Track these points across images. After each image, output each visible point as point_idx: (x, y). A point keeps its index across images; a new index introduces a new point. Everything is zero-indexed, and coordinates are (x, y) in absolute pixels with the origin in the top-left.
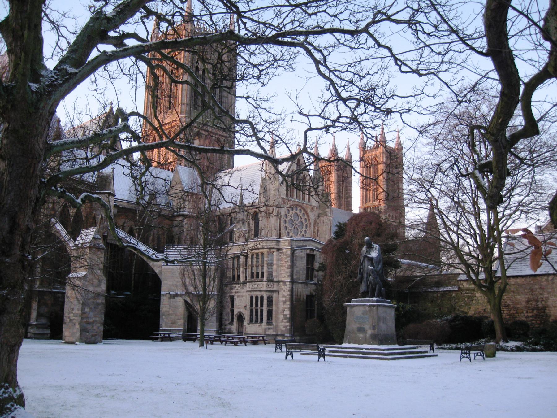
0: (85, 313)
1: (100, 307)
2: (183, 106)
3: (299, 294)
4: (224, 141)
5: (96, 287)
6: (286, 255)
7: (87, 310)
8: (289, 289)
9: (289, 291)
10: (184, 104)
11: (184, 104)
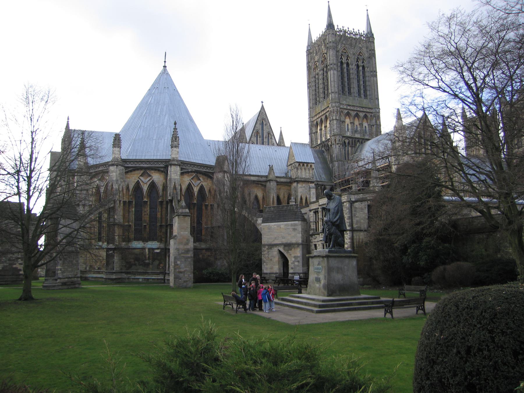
0: (178, 265)
1: (189, 260)
2: (333, 94)
3: (361, 241)
4: (371, 116)
5: (185, 245)
6: (346, 208)
7: (179, 262)
9: (350, 239)
10: (333, 93)
11: (333, 93)
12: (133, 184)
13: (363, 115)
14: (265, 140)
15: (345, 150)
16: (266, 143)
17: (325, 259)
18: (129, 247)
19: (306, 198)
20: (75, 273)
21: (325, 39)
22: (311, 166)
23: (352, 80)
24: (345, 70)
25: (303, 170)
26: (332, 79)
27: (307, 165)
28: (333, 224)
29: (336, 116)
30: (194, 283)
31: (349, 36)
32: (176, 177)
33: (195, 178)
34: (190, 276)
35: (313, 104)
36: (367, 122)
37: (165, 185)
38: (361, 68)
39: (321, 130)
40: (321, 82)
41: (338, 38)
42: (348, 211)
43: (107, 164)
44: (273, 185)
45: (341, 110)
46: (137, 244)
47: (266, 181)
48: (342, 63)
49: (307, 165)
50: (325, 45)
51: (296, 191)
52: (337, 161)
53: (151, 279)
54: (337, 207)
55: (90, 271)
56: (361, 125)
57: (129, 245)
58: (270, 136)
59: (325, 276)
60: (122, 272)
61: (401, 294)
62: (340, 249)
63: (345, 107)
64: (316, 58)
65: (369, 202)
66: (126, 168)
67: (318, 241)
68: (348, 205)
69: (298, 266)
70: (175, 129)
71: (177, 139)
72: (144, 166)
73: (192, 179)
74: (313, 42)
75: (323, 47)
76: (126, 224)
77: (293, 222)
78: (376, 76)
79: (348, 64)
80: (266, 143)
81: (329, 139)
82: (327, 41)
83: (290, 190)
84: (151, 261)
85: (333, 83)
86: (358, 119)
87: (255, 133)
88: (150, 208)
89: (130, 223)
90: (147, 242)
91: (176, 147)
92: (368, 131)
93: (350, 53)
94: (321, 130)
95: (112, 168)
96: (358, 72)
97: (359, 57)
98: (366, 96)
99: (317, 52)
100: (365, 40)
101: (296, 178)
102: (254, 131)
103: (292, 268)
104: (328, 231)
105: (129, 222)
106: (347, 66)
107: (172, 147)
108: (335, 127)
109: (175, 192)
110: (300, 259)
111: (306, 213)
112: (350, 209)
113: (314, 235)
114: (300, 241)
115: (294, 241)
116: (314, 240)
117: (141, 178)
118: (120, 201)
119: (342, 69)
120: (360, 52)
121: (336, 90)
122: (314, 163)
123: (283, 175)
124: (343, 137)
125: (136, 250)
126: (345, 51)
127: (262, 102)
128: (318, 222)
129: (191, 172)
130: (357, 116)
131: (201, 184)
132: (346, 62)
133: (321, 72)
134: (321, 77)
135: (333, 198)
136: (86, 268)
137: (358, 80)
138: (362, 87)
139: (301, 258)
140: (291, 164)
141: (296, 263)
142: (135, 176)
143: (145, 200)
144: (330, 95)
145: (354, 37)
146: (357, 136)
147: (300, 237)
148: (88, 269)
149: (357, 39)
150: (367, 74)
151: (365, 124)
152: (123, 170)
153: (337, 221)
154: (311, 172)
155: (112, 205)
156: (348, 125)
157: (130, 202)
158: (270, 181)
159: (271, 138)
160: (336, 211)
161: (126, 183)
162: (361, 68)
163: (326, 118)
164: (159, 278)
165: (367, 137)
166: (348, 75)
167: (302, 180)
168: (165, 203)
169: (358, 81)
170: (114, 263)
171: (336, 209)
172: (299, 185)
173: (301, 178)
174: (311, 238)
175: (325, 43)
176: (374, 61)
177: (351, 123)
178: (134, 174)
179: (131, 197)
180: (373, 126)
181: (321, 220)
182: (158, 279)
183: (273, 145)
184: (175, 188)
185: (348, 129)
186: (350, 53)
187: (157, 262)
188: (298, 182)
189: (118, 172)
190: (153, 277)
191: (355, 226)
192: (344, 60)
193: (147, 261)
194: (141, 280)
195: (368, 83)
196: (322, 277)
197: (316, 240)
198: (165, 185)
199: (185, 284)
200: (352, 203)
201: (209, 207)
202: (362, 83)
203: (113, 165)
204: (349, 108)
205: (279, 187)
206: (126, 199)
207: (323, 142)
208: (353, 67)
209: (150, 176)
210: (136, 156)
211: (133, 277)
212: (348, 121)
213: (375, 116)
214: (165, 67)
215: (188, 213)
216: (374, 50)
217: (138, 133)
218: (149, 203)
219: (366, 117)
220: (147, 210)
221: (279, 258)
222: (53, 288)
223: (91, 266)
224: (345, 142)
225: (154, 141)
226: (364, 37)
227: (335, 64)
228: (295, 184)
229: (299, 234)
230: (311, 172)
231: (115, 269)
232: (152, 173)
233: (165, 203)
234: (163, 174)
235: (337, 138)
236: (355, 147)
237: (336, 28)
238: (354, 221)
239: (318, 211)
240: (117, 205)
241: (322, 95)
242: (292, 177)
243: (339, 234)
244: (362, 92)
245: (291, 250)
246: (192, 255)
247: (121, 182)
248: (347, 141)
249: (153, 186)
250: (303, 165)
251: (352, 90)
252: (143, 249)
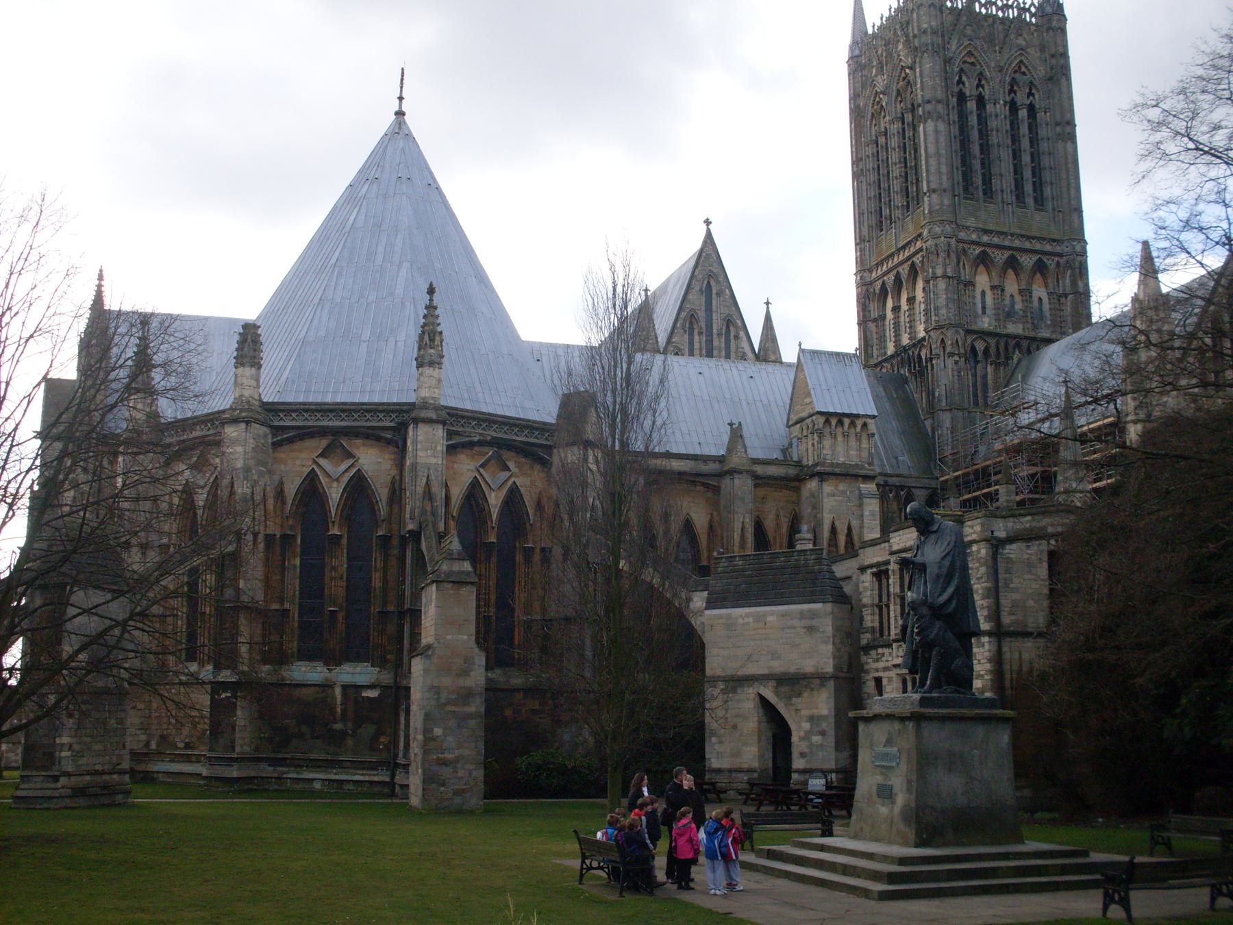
0: (434, 739)
1: (472, 723)
2: (934, 196)
3: (1025, 668)
4: (1058, 264)
5: (459, 675)
6: (978, 560)
7: (438, 731)
8: (987, 654)
9: (990, 661)
10: (934, 191)
11: (934, 191)
12: (298, 481)
13: (1032, 263)
14: (716, 343)
15: (975, 375)
16: (720, 351)
17: (910, 725)
18: (283, 679)
19: (849, 529)
20: (114, 759)
21: (908, 23)
22: (865, 425)
23: (994, 152)
24: (973, 120)
25: (840, 438)
26: (931, 149)
27: (853, 424)
28: (937, 612)
29: (945, 266)
30: (485, 798)
31: (984, 11)
32: (433, 461)
33: (492, 462)
34: (474, 774)
35: (870, 227)
36: (1046, 286)
37: (397, 486)
38: (1023, 113)
39: (896, 309)
40: (895, 156)
41: (949, 19)
42: (983, 569)
43: (216, 420)
44: (741, 486)
45: (961, 246)
46: (308, 672)
47: (720, 475)
48: (962, 97)
49: (853, 424)
50: (907, 42)
51: (816, 507)
52: (951, 410)
53: (348, 781)
54: (949, 559)
55: (160, 754)
56: (1026, 293)
57: (284, 674)
58: (732, 328)
59: (909, 782)
60: (259, 760)
61: (1157, 843)
62: (959, 692)
63: (974, 237)
64: (881, 82)
65: (1053, 542)
66: (276, 430)
67: (886, 669)
68: (983, 551)
69: (822, 746)
70: (431, 307)
71: (437, 338)
72: (331, 424)
73: (483, 466)
74: (870, 31)
75: (900, 46)
76: (275, 606)
77: (806, 606)
78: (1072, 137)
79: (981, 101)
80: (720, 351)
81: (924, 339)
82: (913, 29)
83: (798, 503)
84: (350, 725)
85: (933, 162)
86: (1017, 275)
87: (685, 320)
88: (350, 559)
89: (287, 606)
90: (339, 664)
91: (431, 364)
92: (1047, 313)
93: (988, 66)
94: (896, 309)
95: (231, 431)
96: (1014, 124)
97: (1017, 76)
98: (1040, 202)
99: (881, 63)
100: (1036, 25)
101: (816, 465)
102: (683, 315)
103: (802, 755)
104: (918, 634)
105: (281, 600)
106: (978, 109)
107: (420, 366)
108: (942, 301)
109: (429, 509)
110: (829, 726)
111: (849, 578)
112: (990, 563)
113: (876, 647)
114: (829, 669)
115: (808, 666)
116: (874, 665)
117: (322, 462)
118: (255, 535)
119: (963, 116)
120: (1021, 62)
121: (946, 184)
122: (874, 417)
123: (776, 455)
124: (969, 332)
125: (304, 690)
126: (972, 60)
127: (708, 222)
128: (888, 606)
129: (481, 443)
130: (1012, 263)
131: (510, 483)
132: (975, 92)
133: (896, 127)
134: (894, 142)
135: (935, 528)
136: (147, 744)
137: (1014, 151)
138: (1027, 173)
139: (832, 720)
140: (801, 421)
141: (816, 739)
142: (304, 455)
143: (335, 531)
144: (926, 199)
145: (1000, 14)
146: (1014, 328)
147: (830, 654)
148: (153, 746)
149: (1012, 21)
150: (1043, 132)
151: (1039, 292)
152: (265, 436)
153: (949, 601)
154: (865, 445)
155: (231, 548)
156: (983, 293)
157: (287, 539)
158: (733, 472)
159: (737, 337)
160: (945, 570)
161: (276, 478)
162: (1023, 113)
163: (914, 272)
164: (376, 779)
165: (1045, 333)
166: (984, 133)
167: (837, 470)
168: (395, 542)
169: (1016, 155)
170: (234, 728)
171: (947, 563)
172: (828, 488)
173: (832, 465)
174: (864, 658)
175: (907, 36)
176: (1064, 89)
177: (993, 288)
178: (300, 451)
179: (291, 522)
180: (1066, 296)
181: (898, 601)
182: (371, 783)
183: (743, 357)
184: (428, 494)
185: (984, 308)
186: (988, 66)
187: (368, 730)
188: (823, 476)
189: (251, 443)
190: (356, 778)
191: (1006, 620)
192: (969, 88)
193: (338, 726)
194: (317, 785)
195: (1046, 161)
196: (898, 782)
197: (881, 665)
198: (397, 486)
199: (457, 800)
200: (996, 545)
201: (537, 557)
202: (1026, 158)
203: (235, 421)
204: (985, 239)
205: (762, 492)
206: (274, 529)
207: (905, 349)
208: (998, 110)
209: (349, 455)
210: (307, 392)
211: (295, 776)
212: (983, 281)
213: (1069, 265)
214: (400, 114)
215: (468, 573)
216: (1065, 55)
217: (315, 322)
218: (344, 542)
219: (1040, 268)
220: (339, 562)
221: (759, 722)
222: (45, 805)
223: (163, 738)
224: (973, 349)
225: (364, 346)
226: (1032, 15)
227: (939, 102)
228: (812, 485)
229: (826, 643)
230: (865, 445)
231: (238, 749)
232: (358, 448)
233: (395, 542)
234: (392, 449)
235: (950, 335)
236: (1006, 365)
238: (1005, 602)
240: (247, 548)
241: (899, 200)
242: (805, 462)
243: (956, 644)
244: (1028, 188)
245: (799, 695)
246: (482, 710)
247: (261, 474)
248: (980, 346)
249: (358, 486)
250: (840, 423)
251: (996, 183)
252: (327, 686)
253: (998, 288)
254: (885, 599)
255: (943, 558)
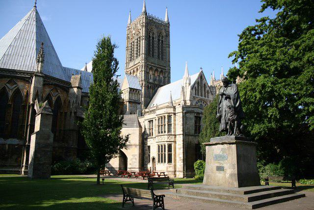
7: (39, 155)
27: (136, 91)
38: (161, 41)
40: (135, 47)
49: (136, 91)
78: (169, 47)
90: (8, 139)
96: (159, 44)
98: (162, 59)
103: (130, 164)
129: (51, 84)
130: (156, 70)
133: (136, 41)
134: (135, 44)
146: (156, 83)
151: (161, 76)
163: (137, 70)
165: (161, 84)
195: (164, 51)
201: (63, 114)
204: (152, 64)
208: (156, 40)
209: (16, 83)
212: (151, 73)
216: (169, 32)
218: (12, 106)
219: (162, 71)
237: (148, 15)
239: (152, 121)
241: (135, 55)
244: (160, 56)
248: (150, 85)
253: (154, 74)
254: (151, 127)
255: (235, 94)
